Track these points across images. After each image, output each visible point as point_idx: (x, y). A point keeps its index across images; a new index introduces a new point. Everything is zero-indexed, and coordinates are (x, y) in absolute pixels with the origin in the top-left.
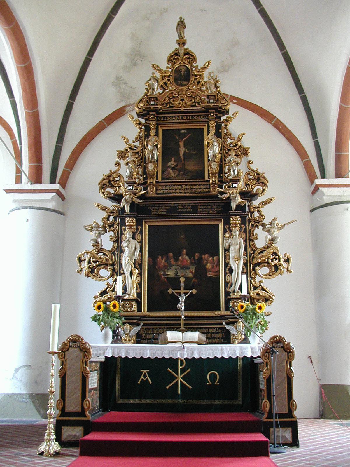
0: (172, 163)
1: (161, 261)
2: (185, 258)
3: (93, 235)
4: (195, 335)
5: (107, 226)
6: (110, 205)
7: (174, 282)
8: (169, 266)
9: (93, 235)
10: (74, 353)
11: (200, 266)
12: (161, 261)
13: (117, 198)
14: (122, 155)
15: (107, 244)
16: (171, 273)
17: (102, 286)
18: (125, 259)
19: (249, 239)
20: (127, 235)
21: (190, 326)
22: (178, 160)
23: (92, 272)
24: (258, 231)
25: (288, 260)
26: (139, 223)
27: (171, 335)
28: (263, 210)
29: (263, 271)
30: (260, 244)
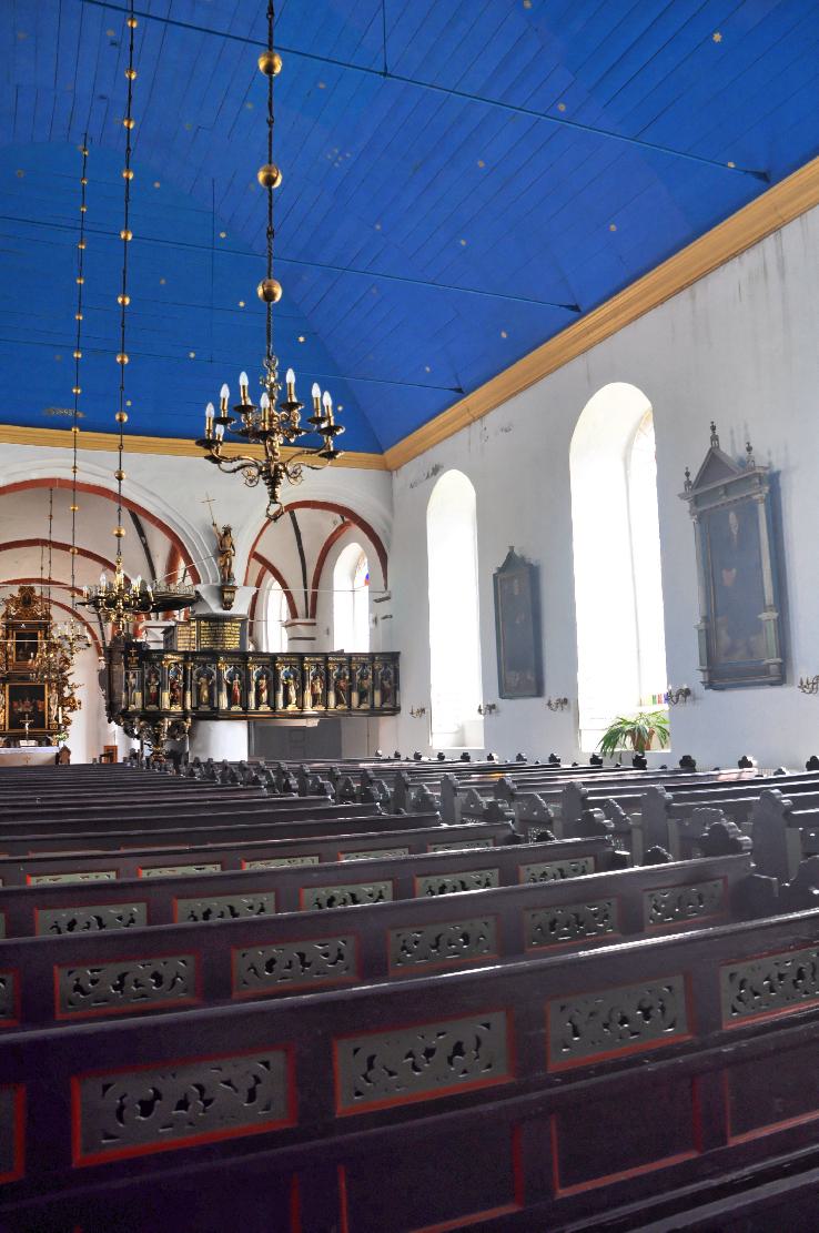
0: (21, 652)
1: (16, 704)
2: (27, 702)
4: (33, 742)
7: (22, 715)
8: (20, 706)
11: (35, 705)
12: (16, 704)
16: (20, 710)
19: (61, 692)
21: (31, 737)
24: (66, 689)
25: (80, 703)
27: (22, 743)
28: (69, 678)
30: (66, 695)
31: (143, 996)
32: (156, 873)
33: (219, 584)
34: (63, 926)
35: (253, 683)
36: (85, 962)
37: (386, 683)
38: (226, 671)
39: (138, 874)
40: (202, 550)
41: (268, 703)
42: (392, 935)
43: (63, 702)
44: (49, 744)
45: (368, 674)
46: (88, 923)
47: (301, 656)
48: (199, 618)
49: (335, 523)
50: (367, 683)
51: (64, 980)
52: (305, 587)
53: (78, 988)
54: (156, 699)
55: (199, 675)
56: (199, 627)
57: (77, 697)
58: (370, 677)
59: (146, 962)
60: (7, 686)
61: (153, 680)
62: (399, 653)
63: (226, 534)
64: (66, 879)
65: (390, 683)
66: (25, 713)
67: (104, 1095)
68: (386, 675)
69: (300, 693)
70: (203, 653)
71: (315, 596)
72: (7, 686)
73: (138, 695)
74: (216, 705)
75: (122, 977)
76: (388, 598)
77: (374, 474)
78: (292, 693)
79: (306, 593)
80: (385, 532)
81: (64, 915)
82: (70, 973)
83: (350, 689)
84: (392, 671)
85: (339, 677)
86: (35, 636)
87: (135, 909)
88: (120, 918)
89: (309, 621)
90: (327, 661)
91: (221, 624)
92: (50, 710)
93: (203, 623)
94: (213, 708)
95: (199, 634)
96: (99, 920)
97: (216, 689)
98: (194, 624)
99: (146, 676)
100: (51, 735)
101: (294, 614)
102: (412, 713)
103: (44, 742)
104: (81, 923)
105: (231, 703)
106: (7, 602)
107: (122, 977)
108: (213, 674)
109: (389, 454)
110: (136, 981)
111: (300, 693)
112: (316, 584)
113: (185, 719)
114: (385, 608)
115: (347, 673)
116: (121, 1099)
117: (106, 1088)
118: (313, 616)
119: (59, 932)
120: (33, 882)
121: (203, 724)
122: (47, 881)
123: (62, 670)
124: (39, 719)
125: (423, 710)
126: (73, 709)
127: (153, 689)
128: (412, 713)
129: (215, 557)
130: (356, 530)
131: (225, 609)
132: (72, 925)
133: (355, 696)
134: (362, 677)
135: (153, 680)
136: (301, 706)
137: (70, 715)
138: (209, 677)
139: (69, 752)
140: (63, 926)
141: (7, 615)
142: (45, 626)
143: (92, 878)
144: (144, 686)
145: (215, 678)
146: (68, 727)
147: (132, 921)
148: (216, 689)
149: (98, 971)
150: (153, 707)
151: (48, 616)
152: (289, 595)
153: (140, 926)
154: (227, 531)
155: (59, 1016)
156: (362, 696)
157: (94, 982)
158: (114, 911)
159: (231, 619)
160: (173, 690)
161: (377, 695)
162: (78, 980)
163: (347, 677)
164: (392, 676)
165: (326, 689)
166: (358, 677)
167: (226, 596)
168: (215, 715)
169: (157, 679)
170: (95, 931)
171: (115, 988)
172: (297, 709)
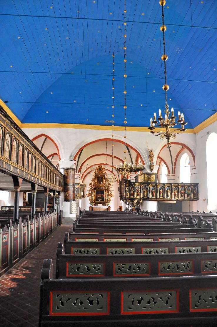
1: (97, 195)
2: (100, 195)
3: (88, 192)
4: (101, 205)
5: (90, 190)
6: (91, 188)
7: (99, 198)
9: (88, 192)
10: (91, 208)
11: (102, 195)
13: (92, 187)
14: (92, 181)
15: (90, 193)
16: (98, 196)
17: (90, 198)
18: (93, 195)
19: (108, 192)
20: (93, 192)
21: (101, 203)
22: (99, 181)
23: (88, 196)
24: (109, 191)
26: (94, 190)
28: (110, 189)
29: (110, 196)
30: (110, 193)
31: (135, 272)
32: (136, 241)
33: (149, 165)
34: (114, 252)
35: (158, 191)
36: (121, 262)
37: (195, 192)
38: (151, 187)
39: (131, 240)
40: (145, 156)
41: (162, 196)
42: (202, 262)
43: (109, 195)
44: (105, 205)
45: (189, 189)
46: (120, 252)
47: (171, 184)
48: (144, 174)
49: (180, 148)
50: (189, 192)
51: (116, 266)
52: (172, 165)
53: (119, 269)
54: (133, 195)
55: (144, 189)
56: (144, 176)
57: (112, 194)
58: (190, 190)
59: (136, 264)
60: (95, 190)
61: (132, 190)
62: (198, 183)
63: (151, 152)
64: (113, 241)
65: (196, 192)
66: (99, 197)
67: (129, 297)
68: (195, 189)
69: (171, 193)
70: (145, 183)
71: (175, 168)
72: (95, 190)
73: (129, 194)
74: (148, 197)
75: (130, 267)
76: (195, 168)
77: (192, 134)
78: (169, 194)
79: (172, 167)
80: (194, 150)
81: (114, 250)
82: (117, 265)
83: (185, 193)
84: (196, 188)
85: (182, 190)
86: (102, 178)
87: (132, 249)
88: (128, 252)
89: (173, 174)
90: (178, 185)
91: (150, 175)
92: (105, 197)
93: (145, 175)
94: (148, 197)
95: (144, 178)
96: (123, 252)
97: (148, 192)
98: (143, 175)
99: (131, 189)
100: (106, 203)
101: (169, 172)
102: (202, 200)
103: (104, 205)
104: (118, 252)
105: (153, 196)
106: (96, 169)
107: (130, 267)
108: (148, 188)
109: (195, 129)
110: (134, 268)
111: (171, 193)
112: (175, 165)
113: (140, 200)
114: (194, 171)
115: (184, 189)
116: (133, 299)
117: (129, 295)
118: (174, 173)
119: (113, 254)
120: (105, 241)
121: (145, 202)
122: (109, 241)
123: (109, 187)
124: (103, 199)
125: (205, 199)
126: (111, 196)
127: (132, 192)
128: (202, 200)
129: (149, 157)
130: (186, 150)
131: (151, 171)
132: (116, 252)
133: (186, 195)
134: (188, 190)
135: (132, 190)
136: (172, 198)
137: (110, 198)
138: (147, 189)
139: (110, 208)
140: (114, 252)
141: (95, 173)
142: (104, 175)
143: (120, 241)
144: (130, 191)
145: (148, 189)
146: (110, 201)
147: (131, 252)
148: (148, 192)
149: (124, 265)
150: (132, 197)
151: (105, 173)
152: (168, 168)
153: (133, 254)
154: (152, 151)
155: (114, 275)
156: (188, 195)
157: (123, 268)
158: (127, 250)
159: (152, 174)
160: (137, 192)
161: (192, 195)
162: (119, 267)
163: (184, 190)
164: (196, 190)
165: (178, 193)
166: (187, 190)
167: (151, 168)
168: (148, 199)
169: (133, 190)
170: (121, 255)
171: (128, 270)
172: (170, 198)
